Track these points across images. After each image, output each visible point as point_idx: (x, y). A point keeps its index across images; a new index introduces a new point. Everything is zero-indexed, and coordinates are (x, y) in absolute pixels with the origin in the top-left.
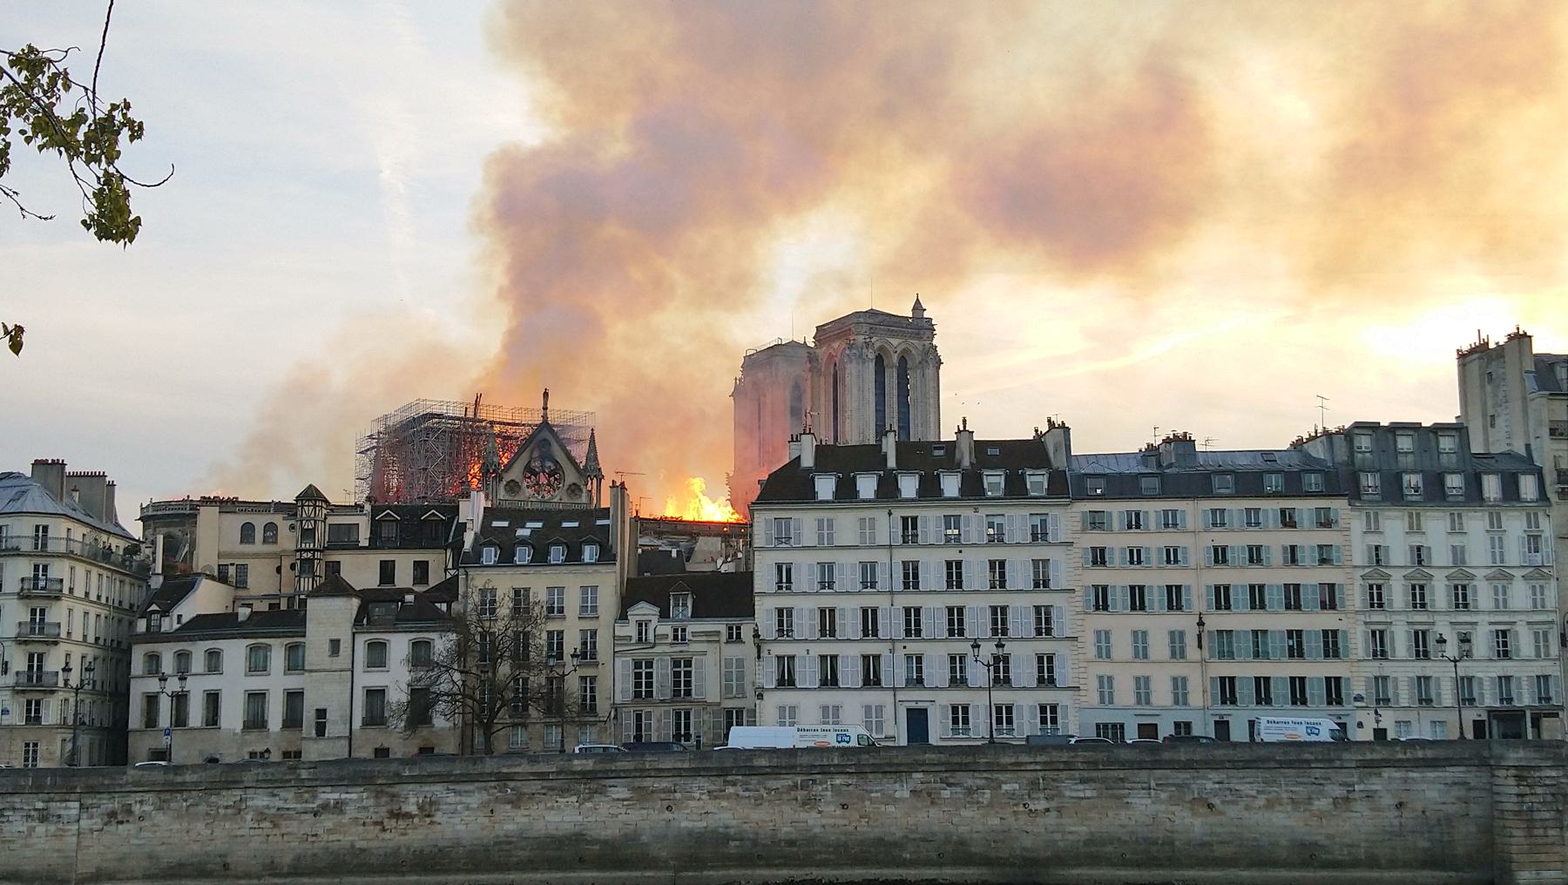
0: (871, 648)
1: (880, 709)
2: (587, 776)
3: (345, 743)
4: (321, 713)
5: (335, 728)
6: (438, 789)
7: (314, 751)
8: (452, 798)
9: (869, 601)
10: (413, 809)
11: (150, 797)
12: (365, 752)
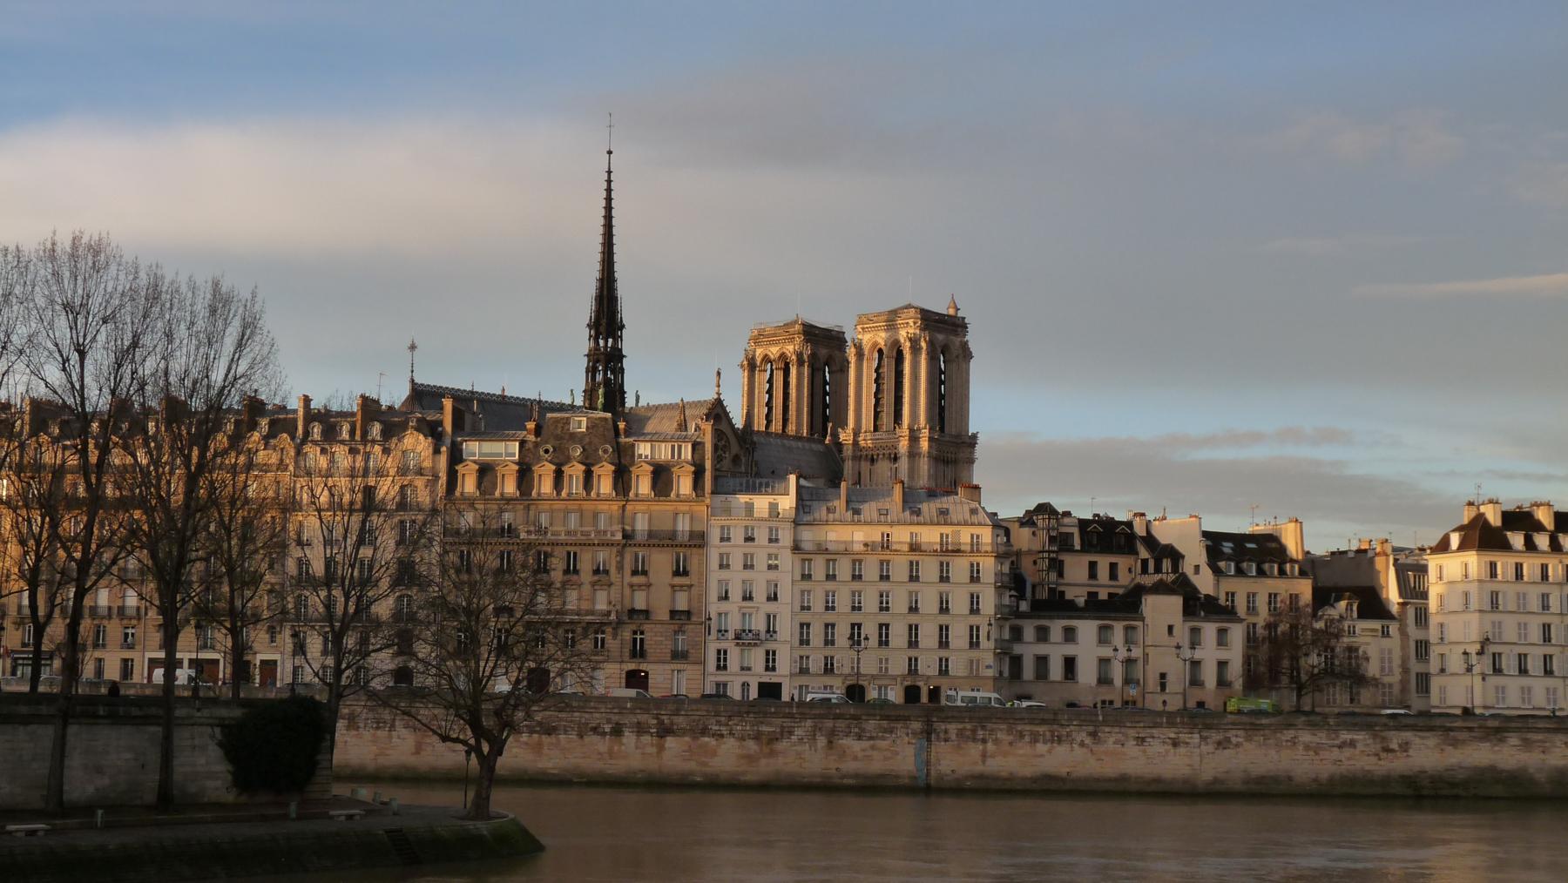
0: (1548, 650)
1: (1555, 690)
2: (1498, 730)
3: (1180, 697)
4: (1163, 676)
5: (1174, 685)
6: (1408, 735)
7: (1155, 702)
8: (1418, 741)
9: (1547, 619)
10: (1394, 746)
11: (1240, 733)
12: (1191, 704)
